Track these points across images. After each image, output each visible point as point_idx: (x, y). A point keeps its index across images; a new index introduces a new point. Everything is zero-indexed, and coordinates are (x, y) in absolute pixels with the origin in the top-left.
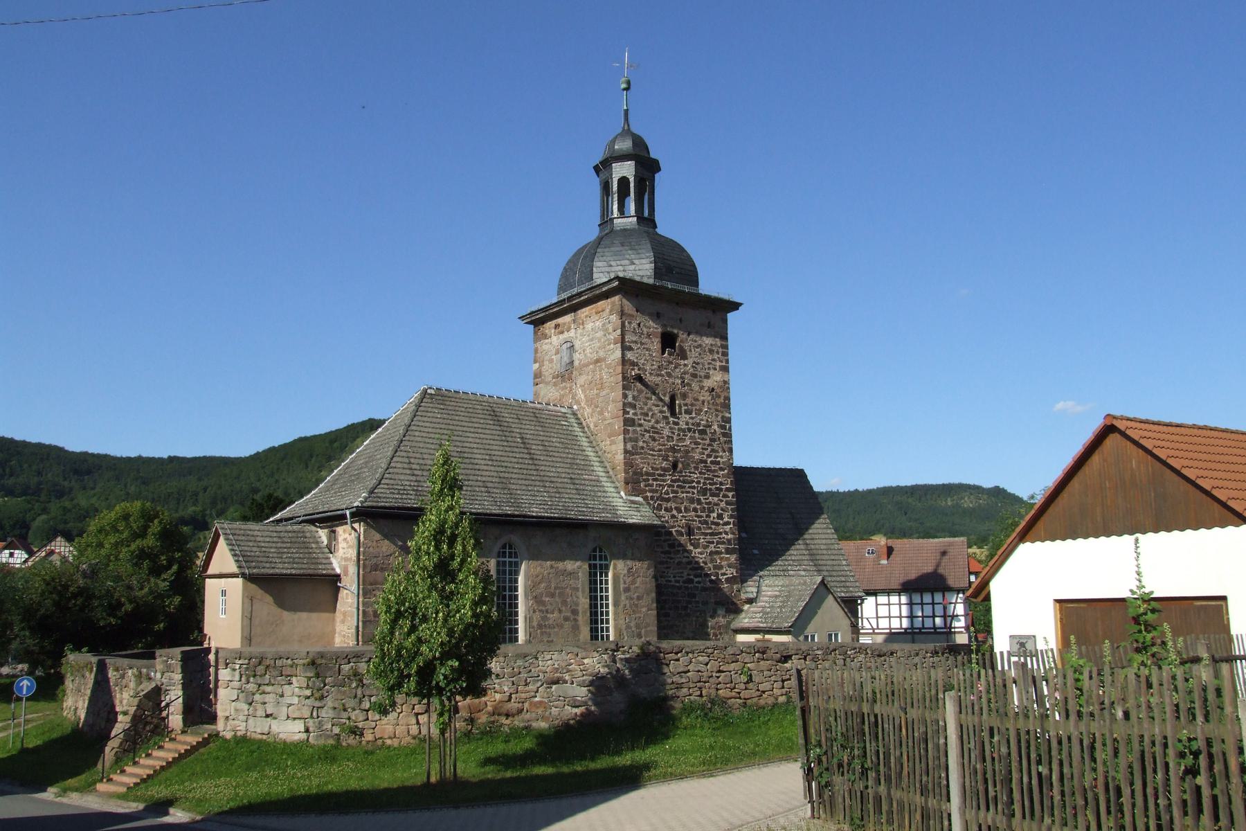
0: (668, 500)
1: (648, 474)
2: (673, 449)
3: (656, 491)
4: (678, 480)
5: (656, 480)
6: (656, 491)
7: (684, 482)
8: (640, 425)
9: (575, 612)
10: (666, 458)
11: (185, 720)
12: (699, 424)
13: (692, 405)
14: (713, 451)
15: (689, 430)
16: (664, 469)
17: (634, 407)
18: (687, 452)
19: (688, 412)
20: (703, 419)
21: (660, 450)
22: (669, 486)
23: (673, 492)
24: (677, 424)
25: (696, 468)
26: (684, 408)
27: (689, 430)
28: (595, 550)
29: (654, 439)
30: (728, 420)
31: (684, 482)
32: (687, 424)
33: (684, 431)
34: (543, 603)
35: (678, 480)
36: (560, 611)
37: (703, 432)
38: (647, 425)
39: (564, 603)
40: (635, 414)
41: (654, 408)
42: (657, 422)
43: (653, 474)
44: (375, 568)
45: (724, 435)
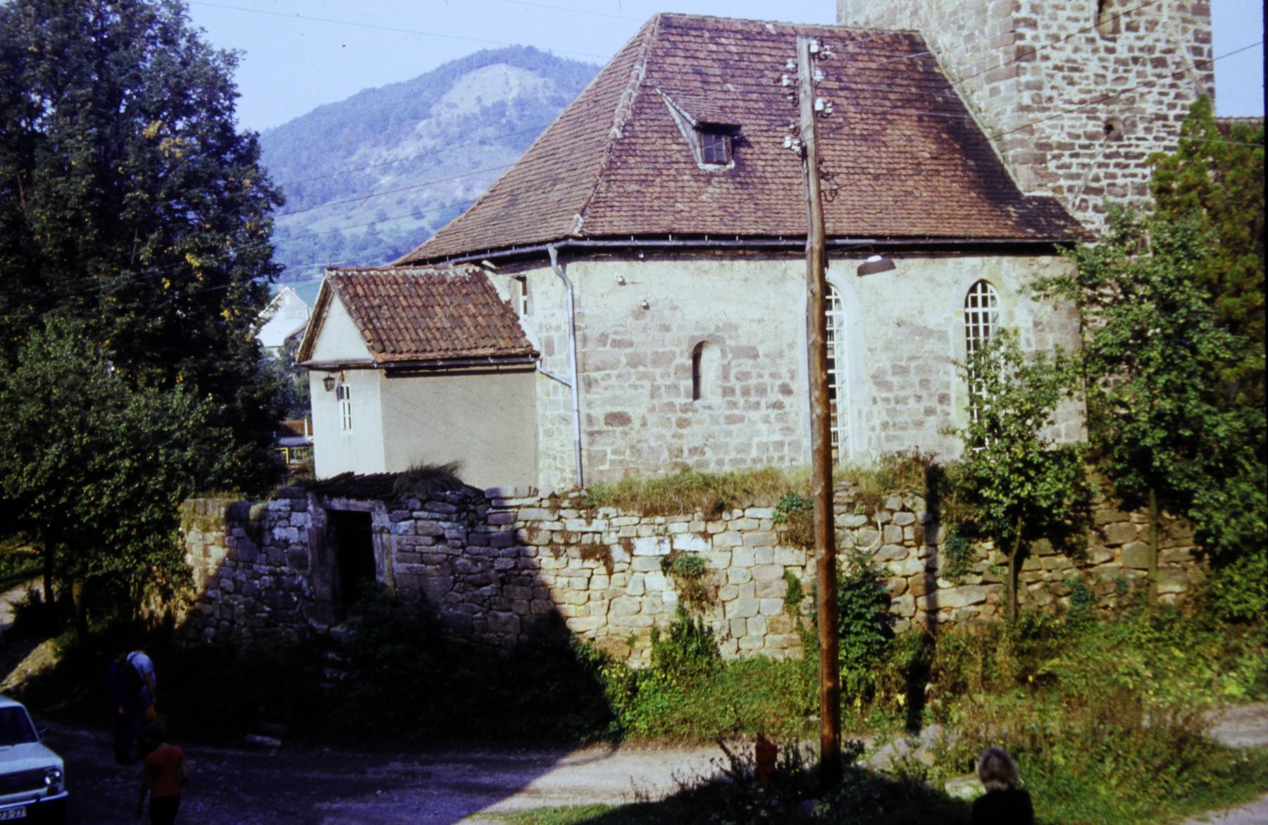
0: (1099, 191)
1: (1061, 146)
2: (1105, 99)
3: (1078, 176)
4: (1116, 154)
5: (1076, 155)
6: (1078, 176)
7: (1127, 156)
8: (1046, 58)
9: (943, 399)
10: (1092, 115)
11: (370, 521)
12: (1151, 49)
13: (1139, 13)
14: (1178, 96)
15: (1135, 60)
16: (1092, 136)
17: (1033, 25)
18: (1131, 101)
19: (1129, 28)
20: (1157, 39)
21: (1082, 102)
22: (1100, 165)
23: (1108, 176)
24: (1111, 51)
25: (1148, 130)
26: (1124, 20)
27: (1135, 60)
28: (973, 289)
29: (1071, 83)
30: (1206, 39)
31: (1127, 156)
32: (1131, 49)
33: (1123, 62)
34: (887, 386)
35: (1116, 154)
36: (919, 398)
37: (1159, 63)
38: (1057, 57)
39: (924, 383)
40: (1035, 38)
41: (1070, 25)
42: (1076, 50)
43: (1071, 146)
44: (958, 768)
45: (1200, 65)
